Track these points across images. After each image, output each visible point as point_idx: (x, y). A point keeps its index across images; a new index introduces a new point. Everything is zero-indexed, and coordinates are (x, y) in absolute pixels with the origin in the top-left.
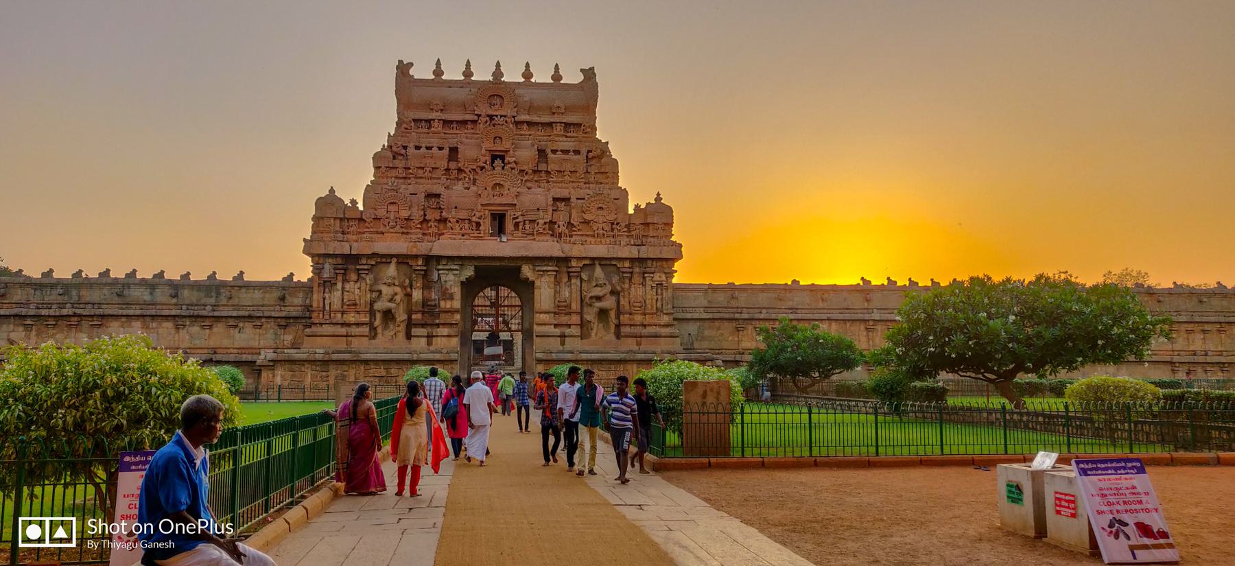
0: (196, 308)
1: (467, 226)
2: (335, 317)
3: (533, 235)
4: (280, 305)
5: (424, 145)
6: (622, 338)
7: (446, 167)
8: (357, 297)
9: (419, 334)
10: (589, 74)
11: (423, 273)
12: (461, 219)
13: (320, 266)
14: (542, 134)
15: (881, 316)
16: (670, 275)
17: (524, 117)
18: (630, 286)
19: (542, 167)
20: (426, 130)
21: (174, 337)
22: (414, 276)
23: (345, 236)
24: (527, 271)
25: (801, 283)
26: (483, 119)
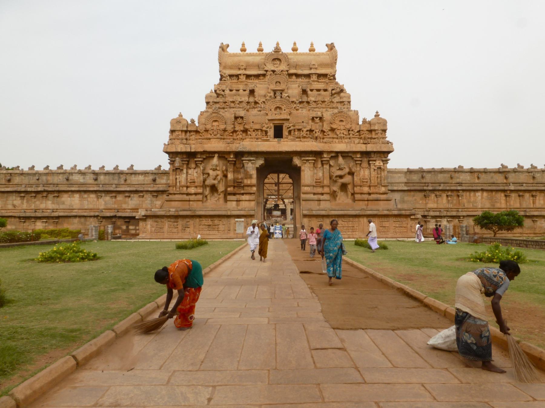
0: (107, 186)
1: (259, 133)
2: (182, 190)
4: (154, 184)
5: (235, 89)
6: (356, 202)
7: (247, 101)
8: (195, 178)
9: (231, 199)
10: (331, 47)
11: (234, 162)
13: (173, 159)
15: (515, 188)
17: (292, 71)
19: (305, 99)
20: (236, 81)
22: (228, 164)
24: (297, 161)
26: (269, 73)
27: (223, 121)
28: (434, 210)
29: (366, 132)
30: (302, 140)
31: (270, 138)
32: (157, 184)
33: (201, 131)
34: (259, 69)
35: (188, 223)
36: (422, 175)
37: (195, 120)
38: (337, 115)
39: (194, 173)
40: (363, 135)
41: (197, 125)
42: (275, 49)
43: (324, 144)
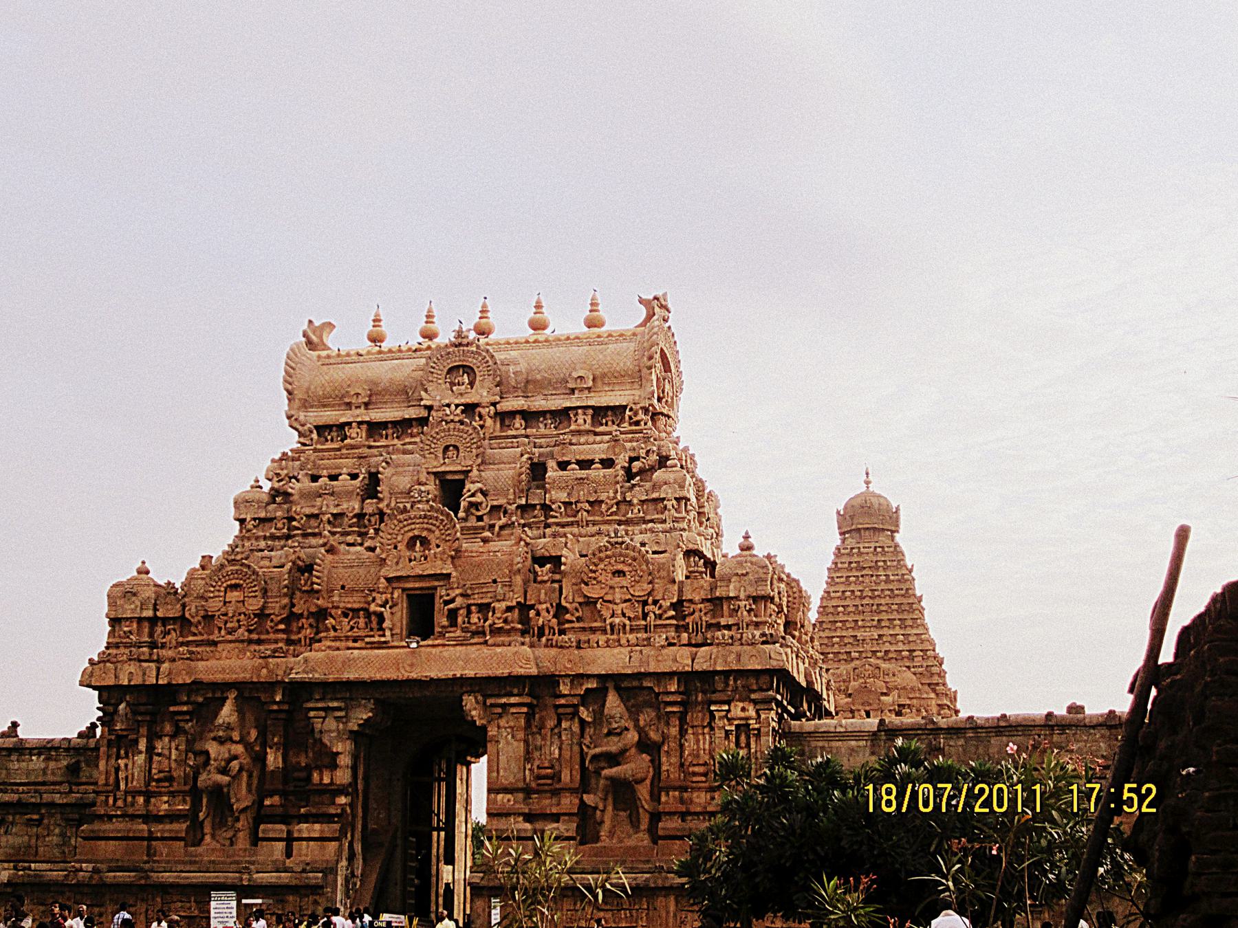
1: (362, 625)
2: (133, 804)
3: (484, 633)
5: (325, 473)
6: (660, 842)
7: (356, 511)
8: (173, 765)
12: (352, 610)
13: (111, 709)
17: (507, 405)
23: (155, 650)
27: (255, 586)
29: (699, 606)
30: (489, 642)
31: (392, 635)
33: (194, 620)
34: (409, 402)
38: (602, 555)
39: (170, 748)
40: (692, 617)
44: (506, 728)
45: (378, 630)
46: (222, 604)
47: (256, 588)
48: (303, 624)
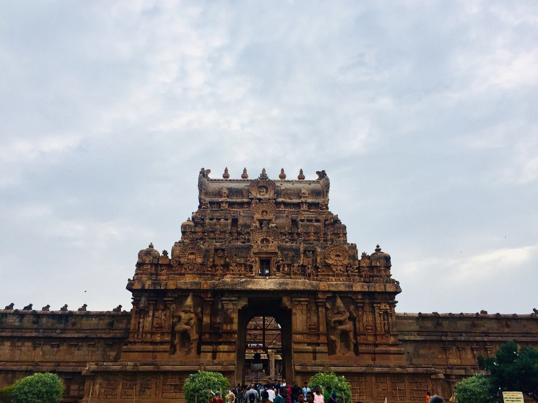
1: (243, 269)
2: (145, 338)
3: (290, 275)
4: (109, 329)
8: (163, 322)
10: (322, 175)
12: (239, 264)
13: (138, 299)
14: (293, 210)
16: (393, 305)
17: (280, 200)
18: (363, 313)
21: (31, 353)
24: (286, 301)
25: (488, 313)
27: (201, 253)
28: (457, 367)
29: (366, 269)
30: (293, 278)
32: (113, 330)
35: (150, 382)
36: (438, 322)
37: (168, 252)
38: (332, 249)
41: (170, 257)
42: (261, 176)
43: (319, 282)
44: (299, 310)
45: (250, 272)
46: (186, 260)
47: (201, 254)
48: (218, 269)
